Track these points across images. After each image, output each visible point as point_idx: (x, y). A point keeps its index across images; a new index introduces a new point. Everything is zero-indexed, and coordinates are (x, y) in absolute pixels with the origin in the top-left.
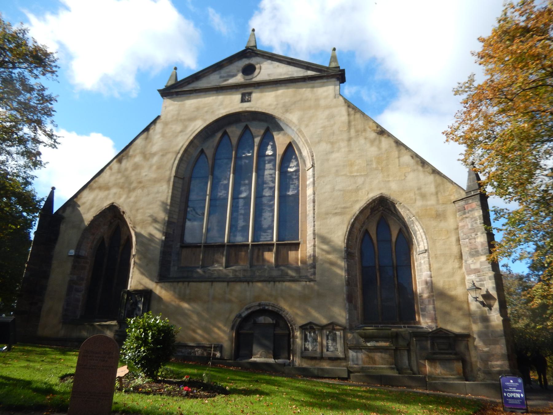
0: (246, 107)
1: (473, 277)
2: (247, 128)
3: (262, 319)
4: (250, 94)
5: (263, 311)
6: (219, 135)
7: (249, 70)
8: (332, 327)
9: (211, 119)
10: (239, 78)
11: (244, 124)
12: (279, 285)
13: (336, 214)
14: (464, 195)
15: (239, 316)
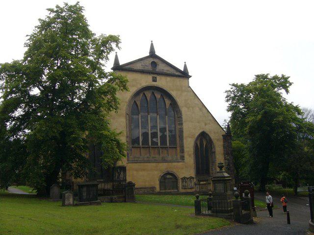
0: (154, 84)
1: (226, 161)
2: (153, 93)
3: (168, 176)
4: (156, 78)
5: (168, 173)
6: (142, 95)
7: (154, 64)
8: (191, 178)
9: (139, 87)
10: (150, 68)
11: (152, 91)
12: (173, 163)
13: (190, 137)
14: (224, 133)
15: (160, 176)
